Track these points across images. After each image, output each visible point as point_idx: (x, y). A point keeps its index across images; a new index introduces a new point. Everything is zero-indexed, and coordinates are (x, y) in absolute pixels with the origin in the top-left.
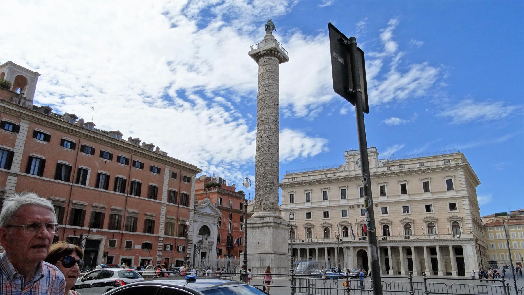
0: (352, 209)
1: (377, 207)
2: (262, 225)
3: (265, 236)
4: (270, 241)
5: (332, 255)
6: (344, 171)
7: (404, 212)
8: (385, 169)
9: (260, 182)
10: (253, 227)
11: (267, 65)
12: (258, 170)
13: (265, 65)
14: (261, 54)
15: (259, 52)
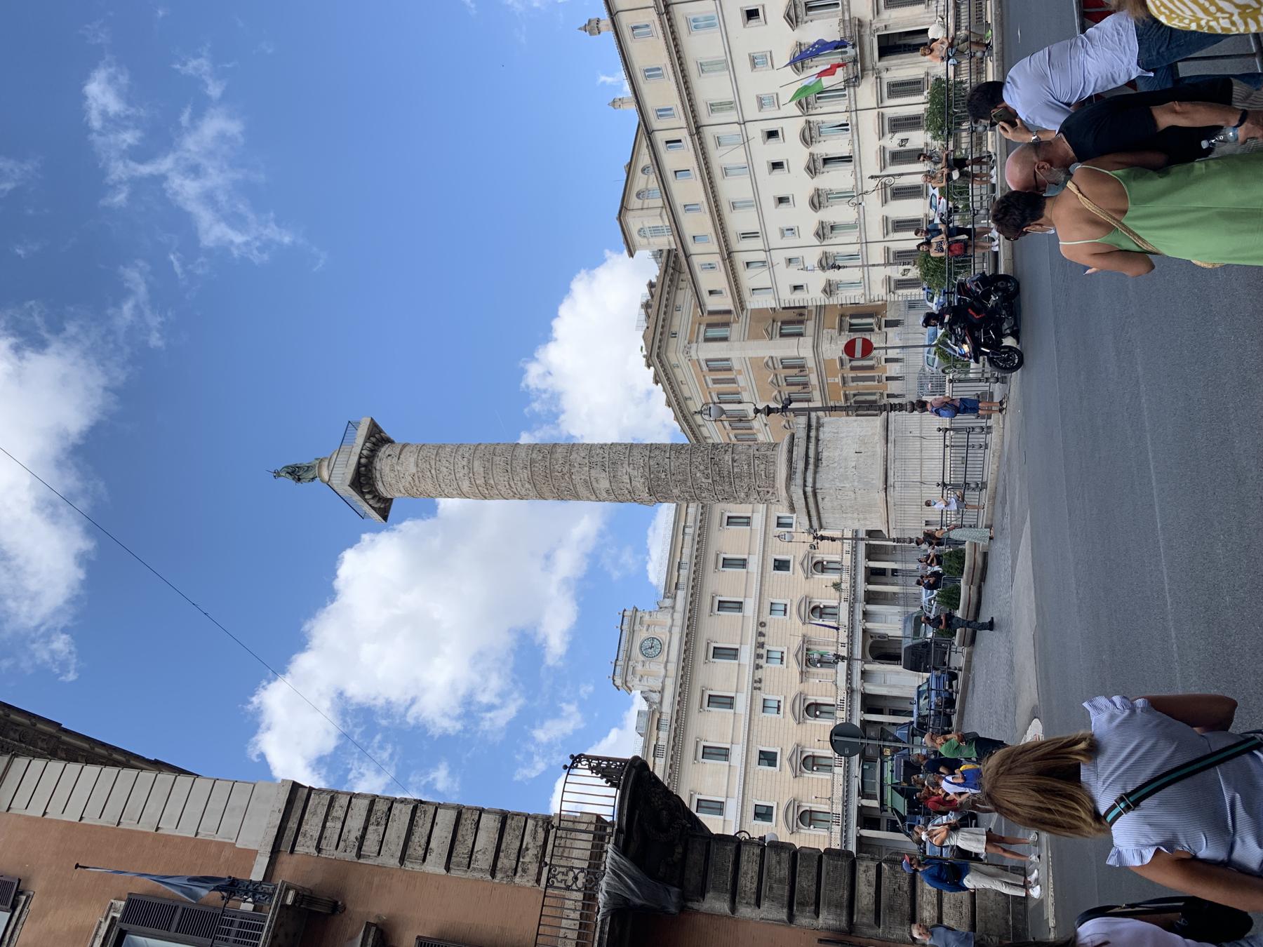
0: (762, 685)
1: (768, 624)
2: (813, 440)
3: (842, 435)
4: (855, 424)
5: (881, 704)
6: (662, 692)
7: (787, 569)
8: (681, 594)
9: (700, 459)
10: (816, 466)
11: (401, 450)
12: (667, 467)
13: (400, 454)
14: (366, 457)
15: (360, 457)
